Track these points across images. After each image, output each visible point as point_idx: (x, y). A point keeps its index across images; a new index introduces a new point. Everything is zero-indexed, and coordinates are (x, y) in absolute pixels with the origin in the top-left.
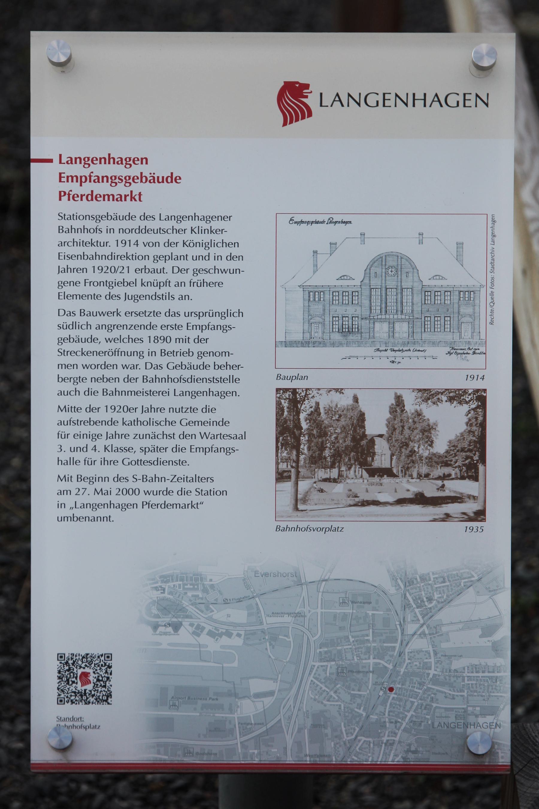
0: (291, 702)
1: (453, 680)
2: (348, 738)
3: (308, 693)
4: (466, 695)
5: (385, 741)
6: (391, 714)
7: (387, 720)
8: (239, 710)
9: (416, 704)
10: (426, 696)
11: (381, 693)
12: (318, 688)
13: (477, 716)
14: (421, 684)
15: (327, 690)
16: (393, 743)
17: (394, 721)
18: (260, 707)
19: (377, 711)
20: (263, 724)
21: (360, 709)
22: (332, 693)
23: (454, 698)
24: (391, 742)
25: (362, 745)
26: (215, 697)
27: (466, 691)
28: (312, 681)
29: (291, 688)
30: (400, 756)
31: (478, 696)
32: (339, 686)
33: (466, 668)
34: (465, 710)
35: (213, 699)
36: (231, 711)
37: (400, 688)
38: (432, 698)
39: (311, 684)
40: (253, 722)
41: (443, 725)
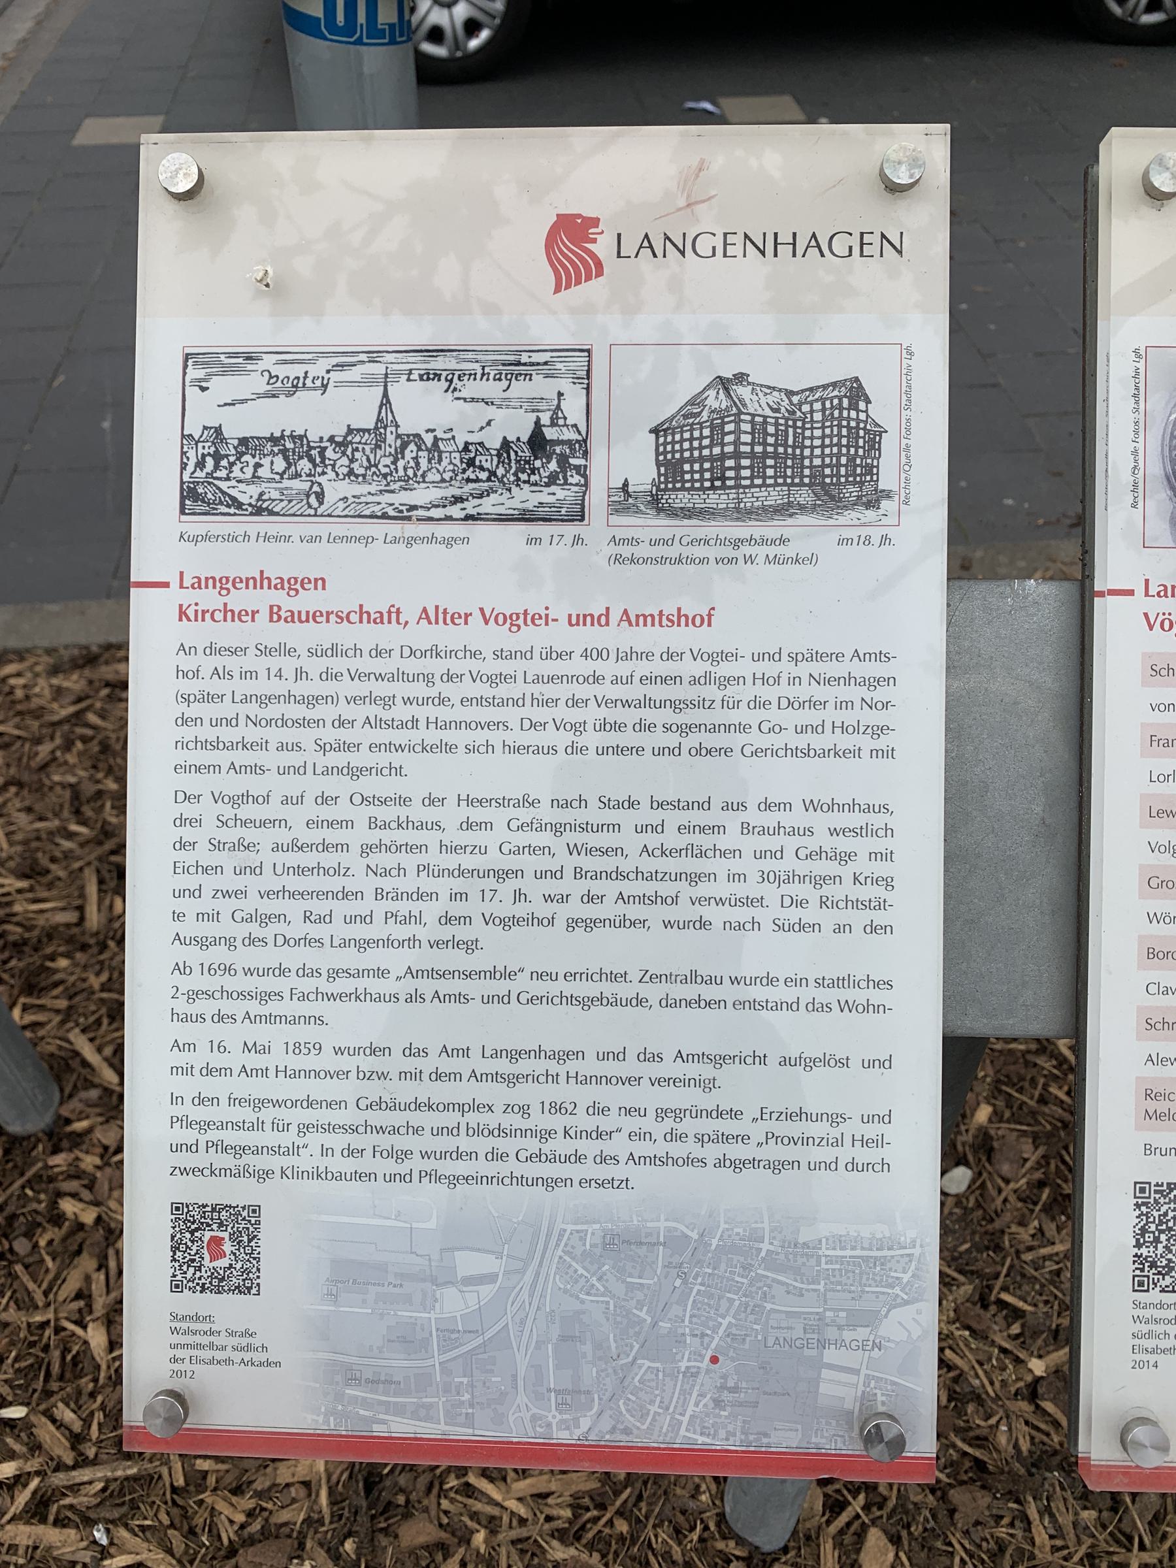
0: (525, 1295)
1: (800, 1260)
4: (822, 1290)
6: (695, 1320)
7: (687, 1330)
8: (437, 1305)
9: (737, 1303)
10: (754, 1289)
11: (678, 1283)
12: (571, 1271)
13: (840, 1328)
14: (747, 1268)
15: (586, 1274)
16: (698, 1373)
21: (641, 1310)
22: (594, 1280)
23: (802, 1295)
24: (694, 1370)
27: (822, 1282)
28: (560, 1257)
29: (523, 1271)
30: (709, 1396)
31: (844, 1291)
32: (606, 1267)
33: (824, 1240)
34: (821, 1317)
38: (765, 1293)
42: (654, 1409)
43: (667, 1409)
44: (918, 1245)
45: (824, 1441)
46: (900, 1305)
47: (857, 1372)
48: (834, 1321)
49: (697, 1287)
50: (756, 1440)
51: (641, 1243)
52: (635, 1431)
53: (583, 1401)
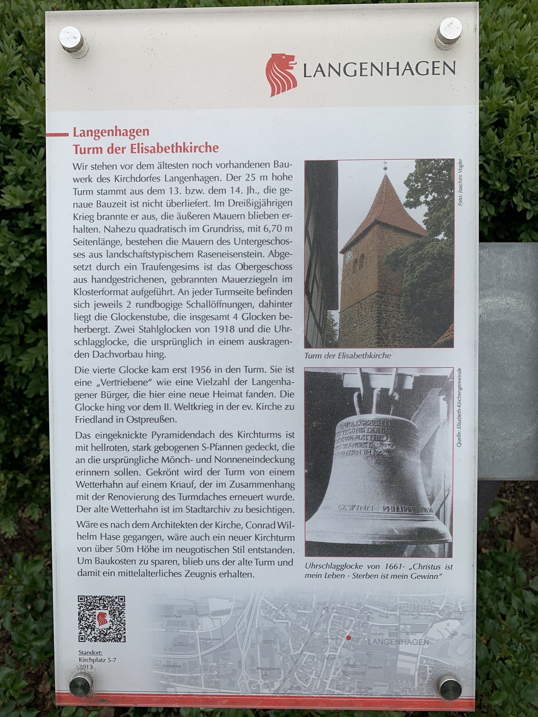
0: (245, 620)
2: (295, 653)
3: (260, 611)
4: (398, 614)
5: (327, 656)
6: (332, 631)
7: (329, 636)
8: (199, 626)
9: (354, 622)
10: (362, 615)
11: (324, 612)
13: (408, 633)
15: (276, 609)
16: (335, 658)
19: (320, 628)
20: (220, 639)
21: (305, 626)
22: (280, 612)
23: (388, 617)
24: (333, 657)
25: (307, 659)
26: (178, 615)
27: (398, 611)
28: (263, 600)
29: (244, 608)
30: (340, 669)
34: (398, 628)
35: (177, 617)
36: (193, 627)
37: (340, 608)
41: (377, 640)
42: (312, 676)
43: (319, 676)
46: (438, 622)
47: (416, 656)
49: (334, 614)
50: (365, 691)
53: (276, 673)
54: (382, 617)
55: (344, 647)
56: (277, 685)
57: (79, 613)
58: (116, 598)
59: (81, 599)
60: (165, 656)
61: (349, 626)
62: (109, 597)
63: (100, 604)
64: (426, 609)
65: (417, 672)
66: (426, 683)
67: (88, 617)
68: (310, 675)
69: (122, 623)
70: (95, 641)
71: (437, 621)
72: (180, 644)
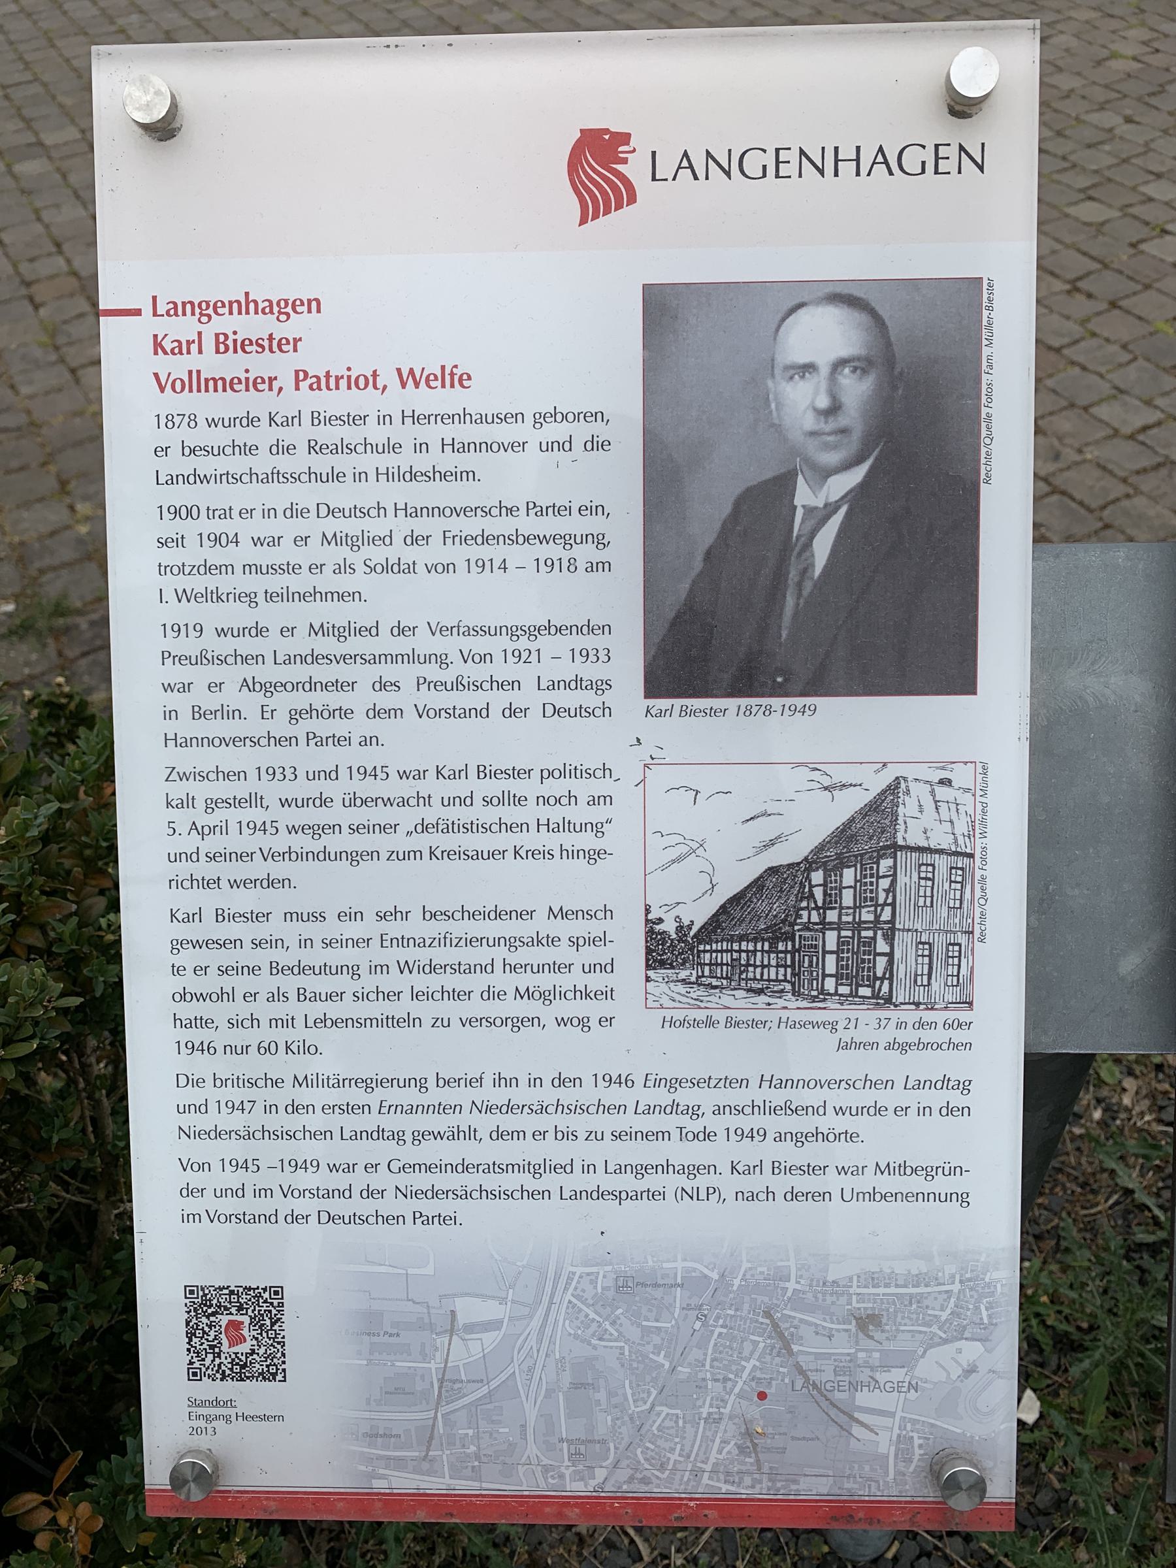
0: (532, 1342)
1: (829, 1299)
2: (639, 1409)
5: (704, 1415)
6: (715, 1363)
7: (709, 1375)
9: (762, 1345)
11: (698, 1325)
12: (583, 1314)
15: (598, 1319)
17: (721, 1377)
18: (475, 1348)
20: (482, 1381)
24: (716, 1416)
26: (395, 1331)
28: (570, 1302)
30: (733, 1443)
32: (620, 1311)
33: (855, 1278)
34: (853, 1358)
37: (732, 1316)
39: (568, 1308)
40: (464, 1378)
43: (689, 1457)
44: (957, 1280)
45: (856, 1486)
46: (939, 1345)
47: (892, 1415)
48: (867, 1362)
49: (719, 1330)
50: (784, 1487)
51: (656, 1285)
52: (654, 1480)
54: (819, 1337)
55: (739, 1396)
56: (601, 1474)
57: (187, 1323)
58: (265, 1290)
59: (192, 1292)
60: (367, 1415)
61: (752, 1353)
62: (250, 1289)
63: (230, 1302)
64: (911, 1319)
65: (893, 1449)
66: (911, 1469)
67: (206, 1329)
68: (668, 1455)
69: (279, 1343)
70: (222, 1380)
71: (932, 1343)
72: (398, 1391)
